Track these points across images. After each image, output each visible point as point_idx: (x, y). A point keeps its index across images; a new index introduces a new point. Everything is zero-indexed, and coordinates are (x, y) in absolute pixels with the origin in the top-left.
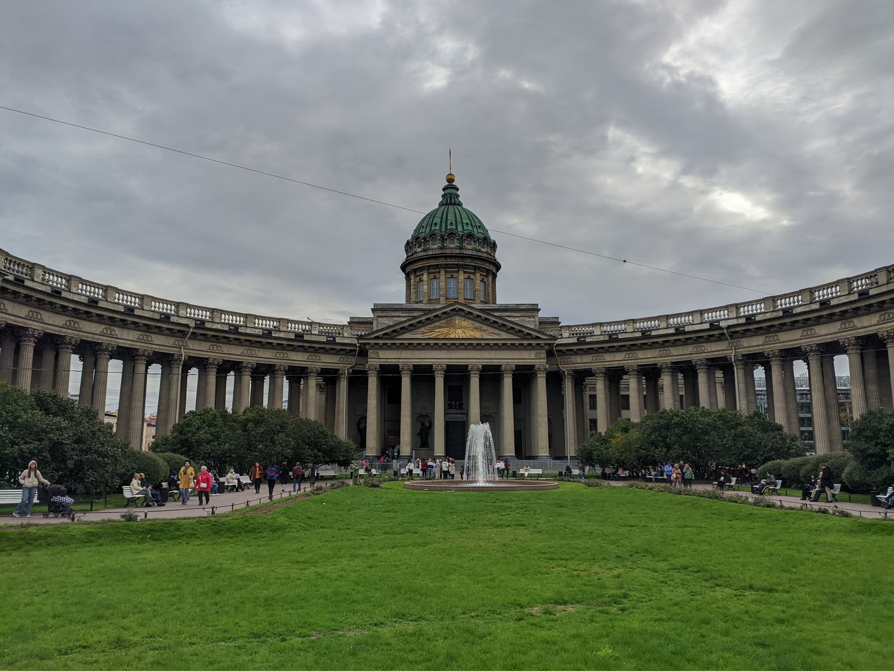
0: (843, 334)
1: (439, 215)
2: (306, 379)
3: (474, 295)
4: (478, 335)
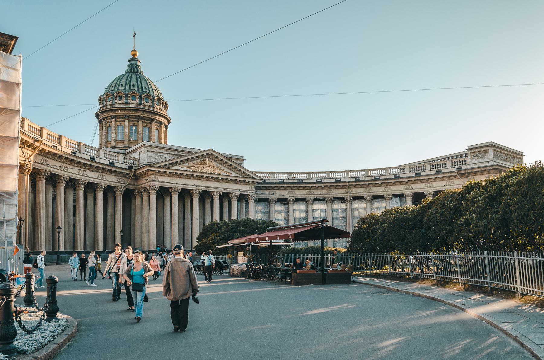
0: (406, 191)
4: (220, 172)
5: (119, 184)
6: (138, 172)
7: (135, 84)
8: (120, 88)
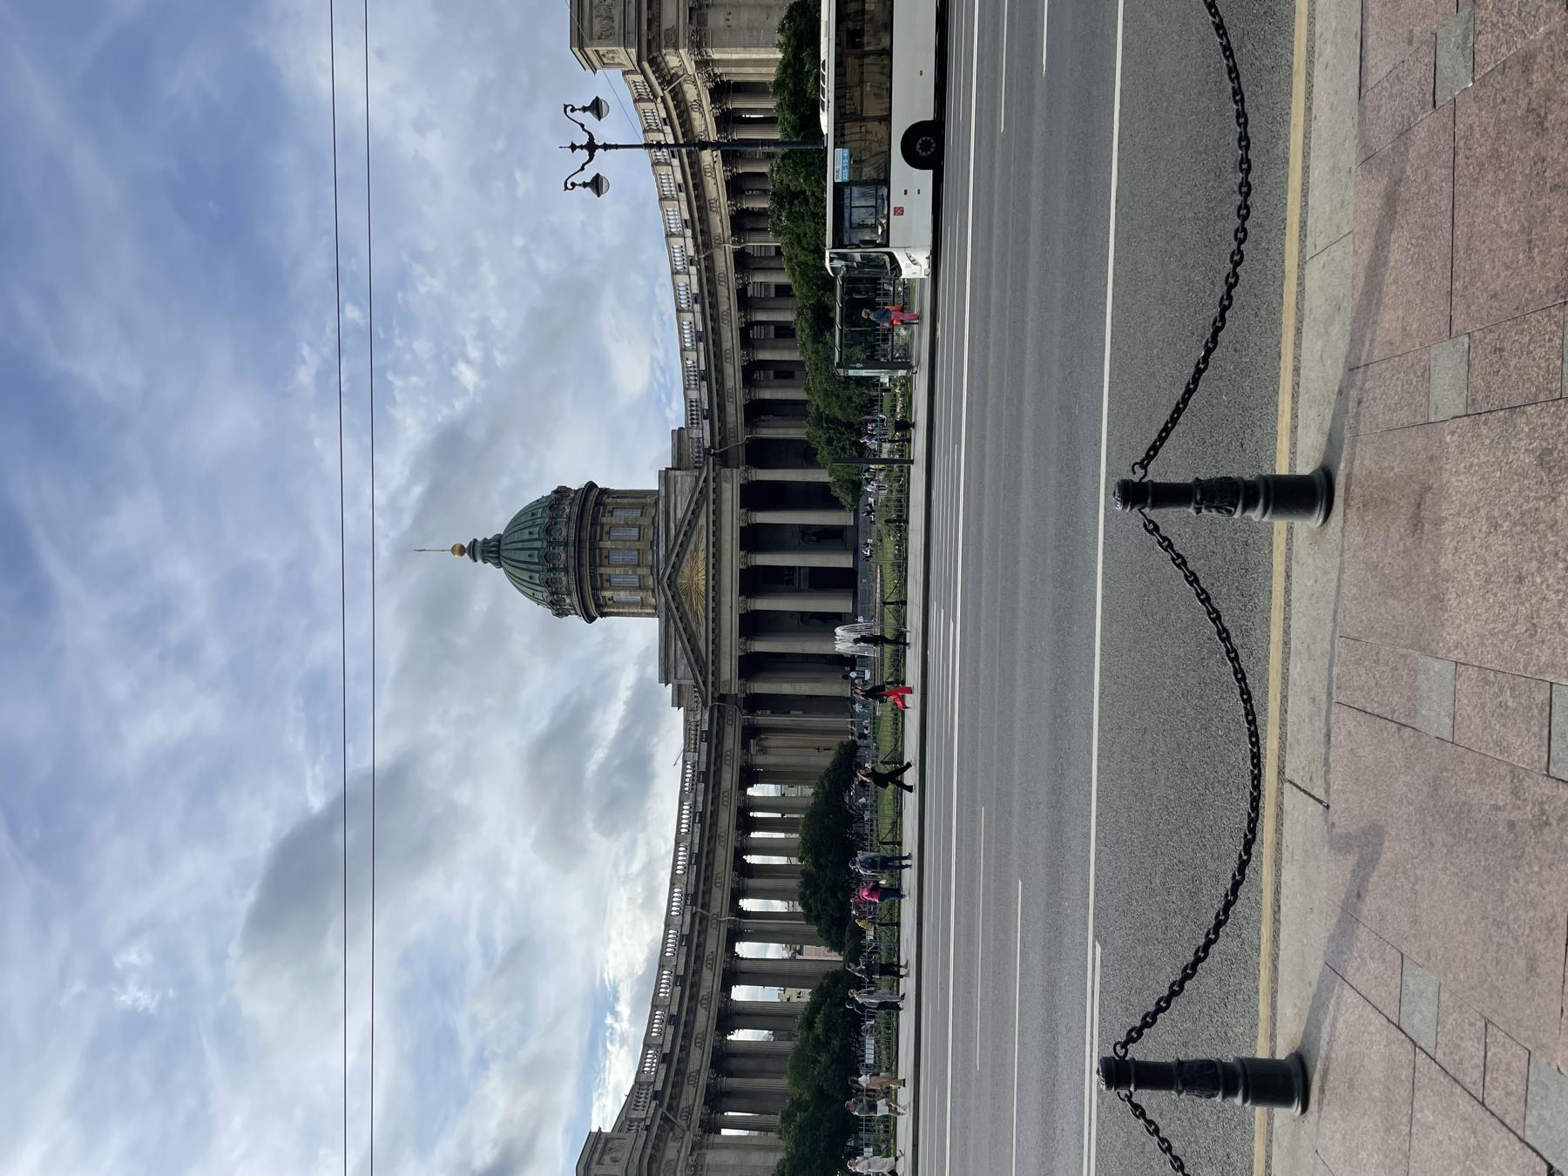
1: (518, 573)
2: (753, 766)
3: (633, 526)
4: (702, 555)
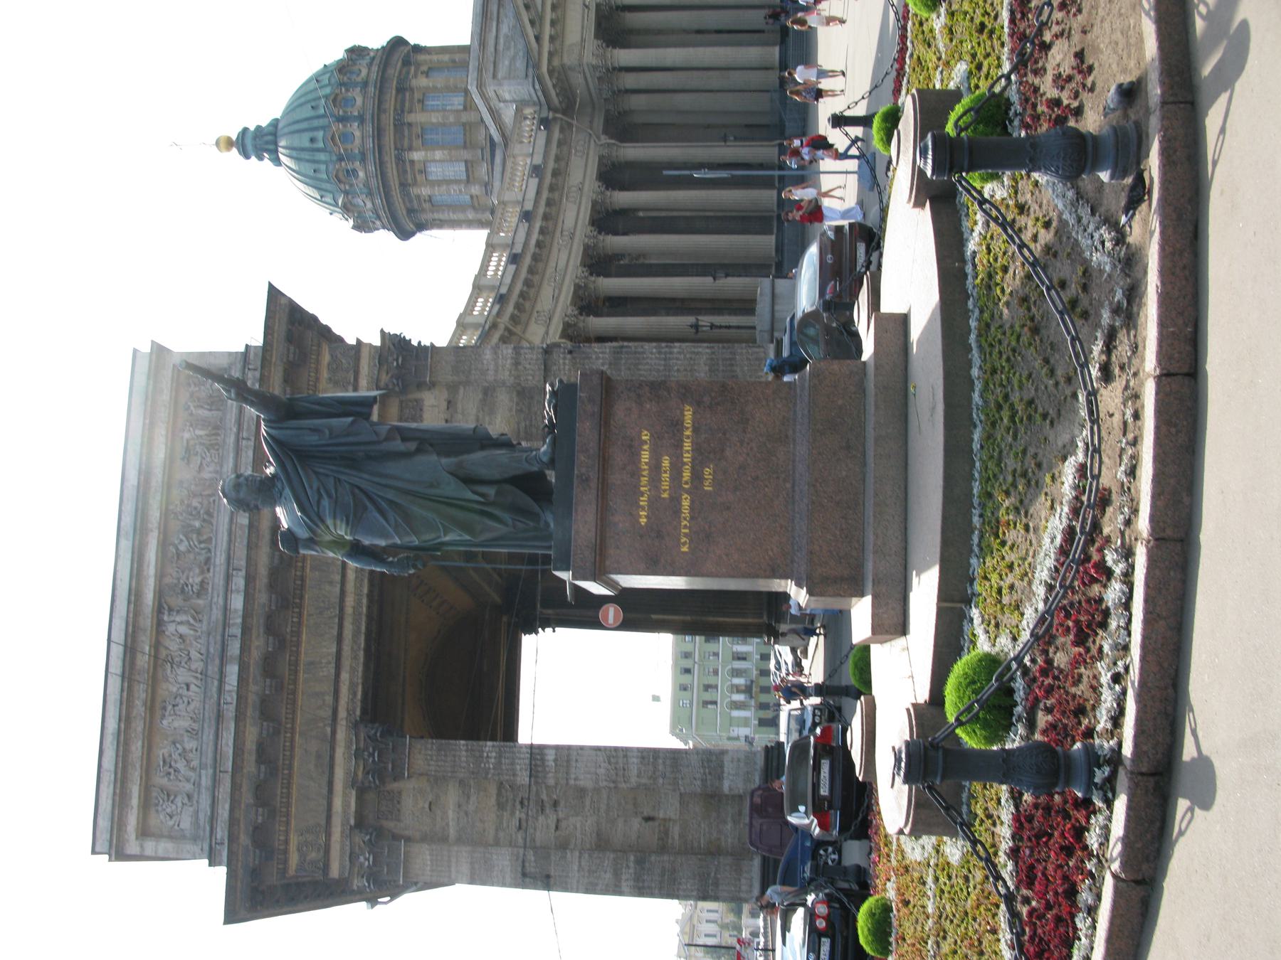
5: (591, 153)
6: (555, 100)
7: (306, 136)
8: (325, 176)
